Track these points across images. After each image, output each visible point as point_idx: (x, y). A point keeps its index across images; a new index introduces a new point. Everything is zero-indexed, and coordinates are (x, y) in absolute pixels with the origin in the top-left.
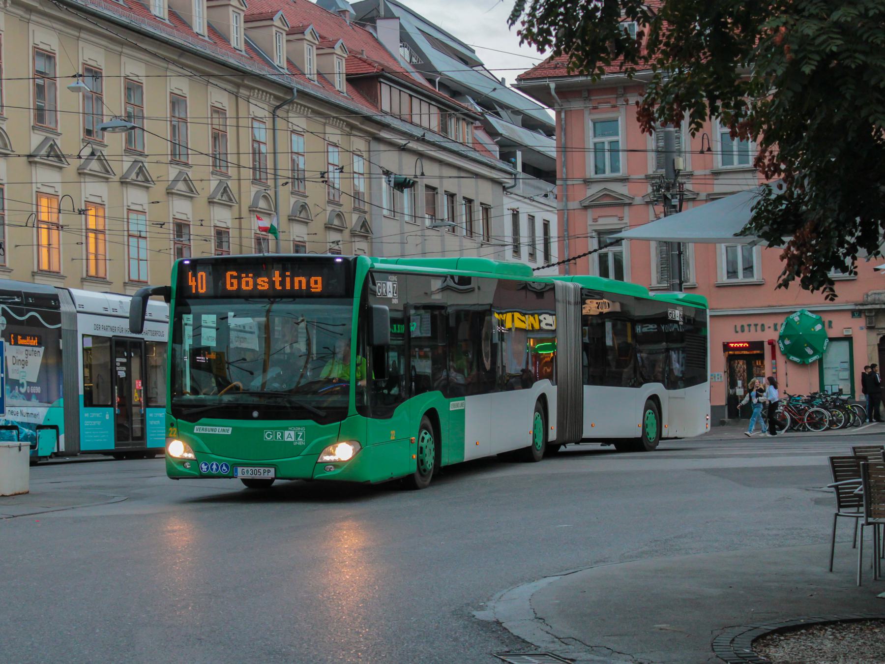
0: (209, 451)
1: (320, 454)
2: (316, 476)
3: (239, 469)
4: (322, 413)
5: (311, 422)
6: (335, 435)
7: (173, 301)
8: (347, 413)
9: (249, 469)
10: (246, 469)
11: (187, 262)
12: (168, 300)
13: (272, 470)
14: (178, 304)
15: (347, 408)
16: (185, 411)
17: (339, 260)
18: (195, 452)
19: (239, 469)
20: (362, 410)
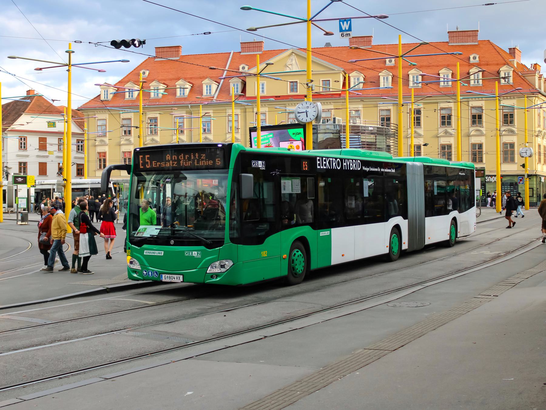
3: (163, 275)
4: (208, 241)
5: (203, 248)
8: (224, 241)
9: (169, 275)
10: (167, 275)
13: (181, 277)
15: (224, 239)
17: (220, 146)
19: (163, 275)
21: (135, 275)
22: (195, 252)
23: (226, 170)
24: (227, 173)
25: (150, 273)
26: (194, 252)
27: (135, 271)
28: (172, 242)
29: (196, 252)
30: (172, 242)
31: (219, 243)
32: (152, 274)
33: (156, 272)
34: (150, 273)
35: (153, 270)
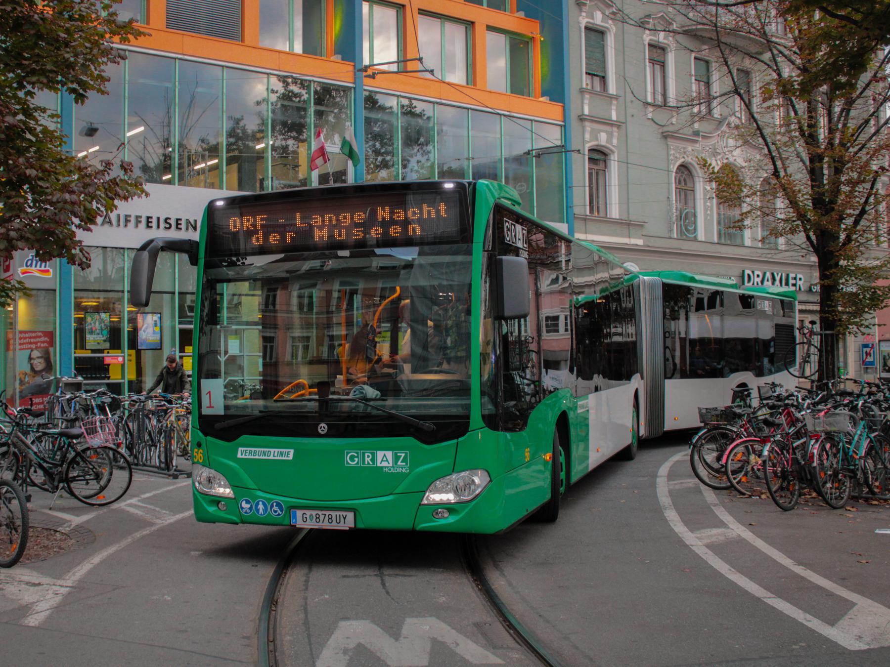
0: (254, 487)
1: (425, 492)
2: (422, 526)
4: (428, 425)
6: (451, 460)
7: (202, 262)
9: (314, 513)
10: (308, 513)
11: (220, 203)
12: (194, 261)
13: (350, 516)
14: (208, 266)
15: (468, 417)
16: (218, 426)
17: (449, 186)
18: (233, 486)
19: (299, 513)
20: (491, 422)
21: (212, 509)
22: (386, 457)
23: (465, 246)
24: (470, 253)
25: (261, 506)
26: (380, 454)
27: (216, 501)
28: (323, 428)
29: (389, 454)
30: (323, 428)
31: (451, 428)
32: (265, 510)
33: (278, 505)
34: (261, 506)
35: (268, 500)
